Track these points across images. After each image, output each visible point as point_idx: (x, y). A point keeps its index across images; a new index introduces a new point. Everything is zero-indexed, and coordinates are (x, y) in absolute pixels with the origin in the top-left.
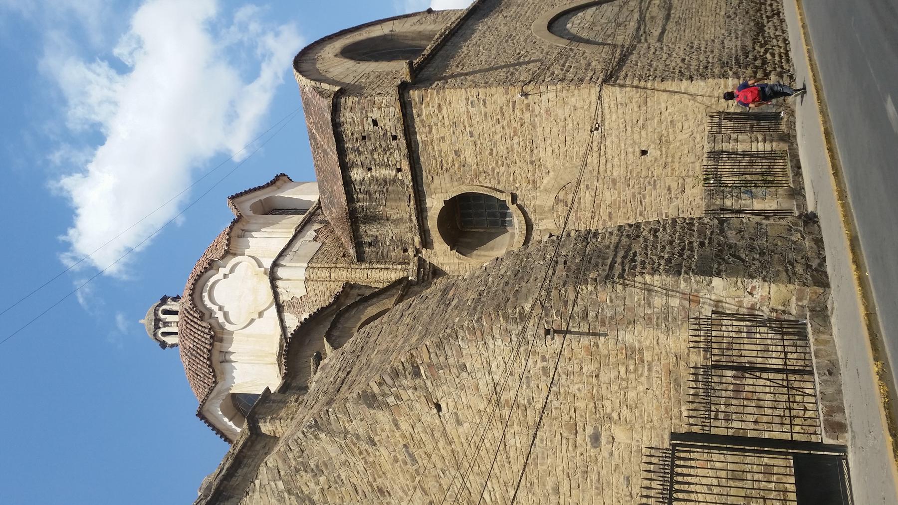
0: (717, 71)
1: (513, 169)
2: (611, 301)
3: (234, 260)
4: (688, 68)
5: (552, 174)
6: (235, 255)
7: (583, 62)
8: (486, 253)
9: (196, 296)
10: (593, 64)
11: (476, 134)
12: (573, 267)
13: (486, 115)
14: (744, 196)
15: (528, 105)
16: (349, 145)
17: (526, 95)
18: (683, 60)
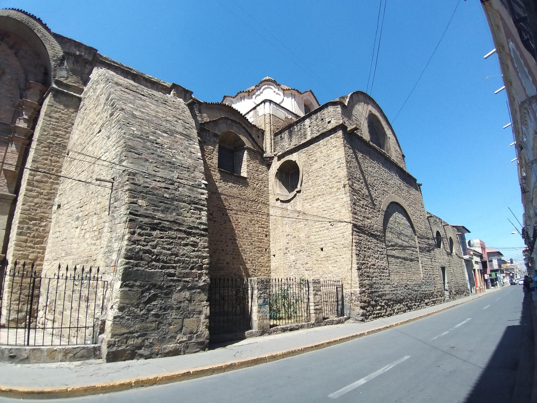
0: (366, 282)
1: (311, 188)
2: (120, 215)
3: (281, 93)
4: (367, 267)
5: (310, 207)
6: (284, 94)
7: (370, 216)
8: (278, 185)
9: (266, 83)
10: (369, 220)
11: (325, 167)
12: (156, 192)
13: (334, 169)
14: (261, 301)
15: (340, 189)
16: (319, 113)
17: (344, 187)
18: (374, 265)
